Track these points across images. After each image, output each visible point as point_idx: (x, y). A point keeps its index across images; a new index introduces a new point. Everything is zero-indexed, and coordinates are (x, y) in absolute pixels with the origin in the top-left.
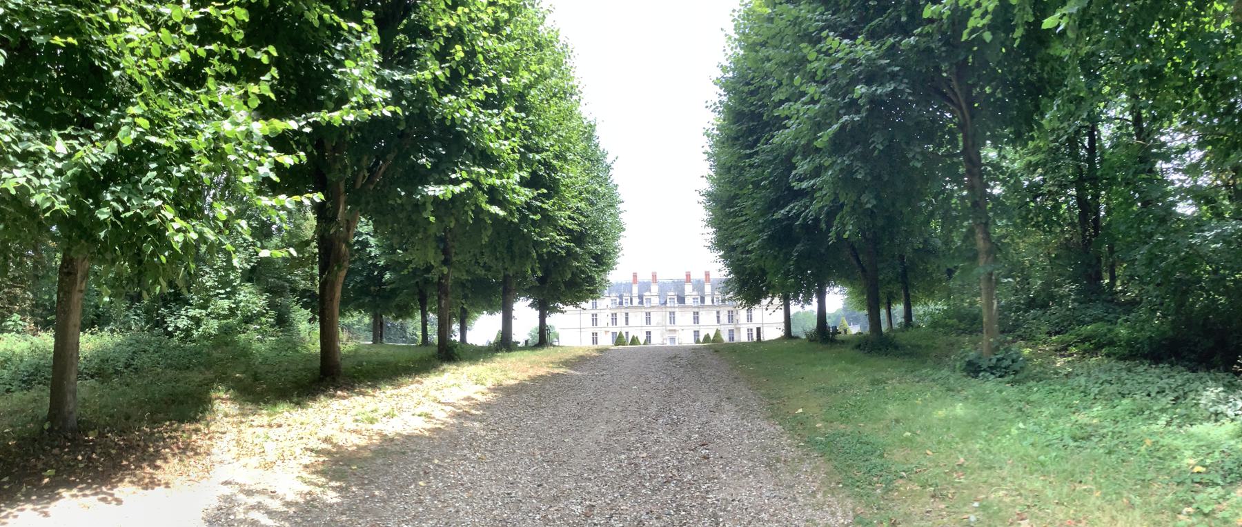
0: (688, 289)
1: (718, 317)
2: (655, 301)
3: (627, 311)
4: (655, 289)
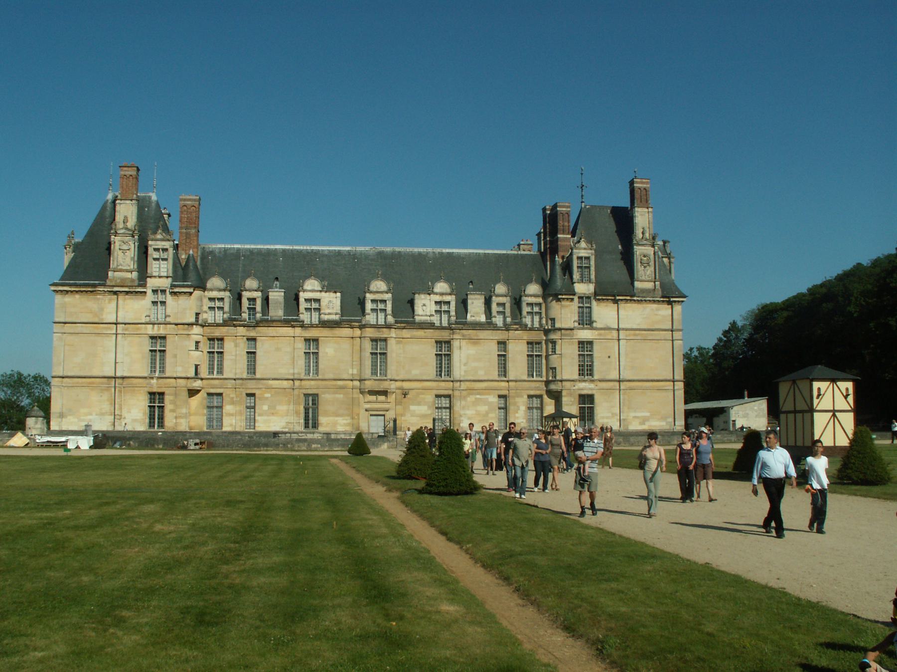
1: (503, 359)
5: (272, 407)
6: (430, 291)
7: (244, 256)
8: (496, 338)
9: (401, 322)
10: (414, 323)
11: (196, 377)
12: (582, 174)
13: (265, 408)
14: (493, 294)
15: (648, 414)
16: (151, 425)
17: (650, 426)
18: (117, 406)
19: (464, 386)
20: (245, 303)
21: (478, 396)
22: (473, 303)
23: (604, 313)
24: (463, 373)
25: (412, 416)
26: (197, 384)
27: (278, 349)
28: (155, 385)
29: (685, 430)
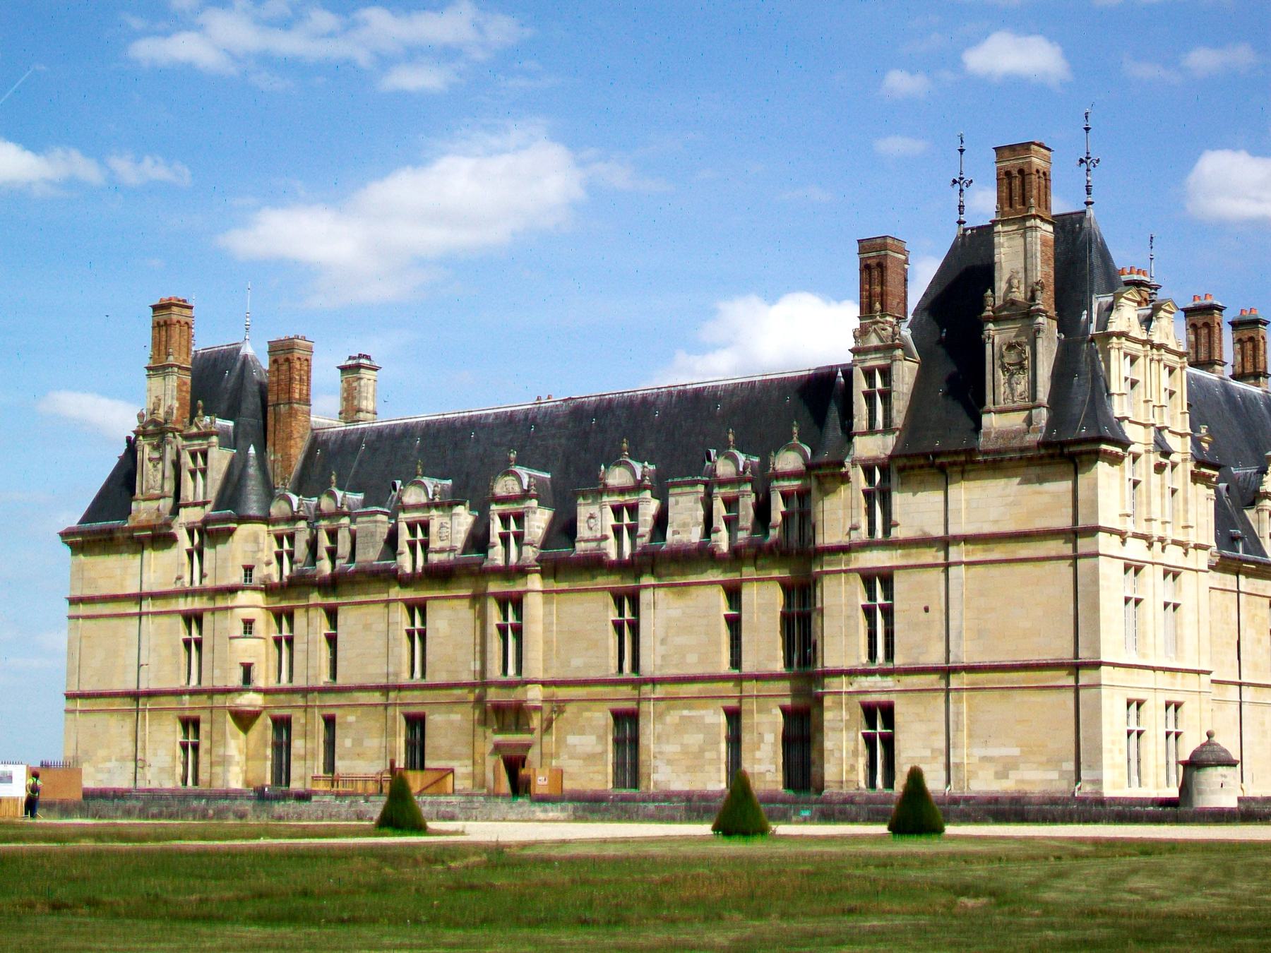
5: (358, 742)
6: (599, 490)
8: (721, 578)
13: (348, 743)
15: (1016, 751)
17: (1022, 781)
18: (139, 744)
19: (660, 691)
21: (686, 713)
22: (677, 503)
24: (659, 662)
25: (571, 758)
27: (367, 627)
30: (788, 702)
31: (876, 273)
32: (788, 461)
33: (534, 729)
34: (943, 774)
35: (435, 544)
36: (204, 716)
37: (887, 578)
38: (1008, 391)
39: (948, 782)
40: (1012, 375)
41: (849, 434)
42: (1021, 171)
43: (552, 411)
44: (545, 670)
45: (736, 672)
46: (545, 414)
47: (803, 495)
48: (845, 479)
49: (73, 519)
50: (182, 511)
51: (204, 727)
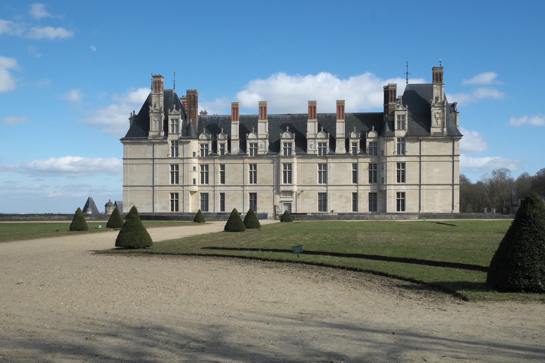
0: (312, 127)
1: (355, 174)
2: (264, 147)
3: (223, 162)
4: (263, 128)
7: (221, 121)
8: (352, 162)
9: (299, 154)
10: (306, 155)
11: (194, 185)
12: (407, 66)
14: (350, 137)
16: (172, 210)
20: (219, 147)
22: (339, 143)
23: (412, 147)
26: (196, 188)
28: (174, 189)
29: (459, 212)
30: (370, 191)
31: (393, 92)
32: (372, 134)
33: (293, 197)
34: (418, 208)
35: (260, 149)
36: (180, 193)
37: (404, 164)
38: (436, 124)
39: (420, 210)
40: (438, 119)
41: (392, 128)
42: (440, 73)
43: (284, 117)
44: (297, 183)
45: (325, 184)
46: (282, 118)
47: (375, 143)
48: (393, 140)
49: (124, 136)
50: (169, 135)
51: (180, 196)
